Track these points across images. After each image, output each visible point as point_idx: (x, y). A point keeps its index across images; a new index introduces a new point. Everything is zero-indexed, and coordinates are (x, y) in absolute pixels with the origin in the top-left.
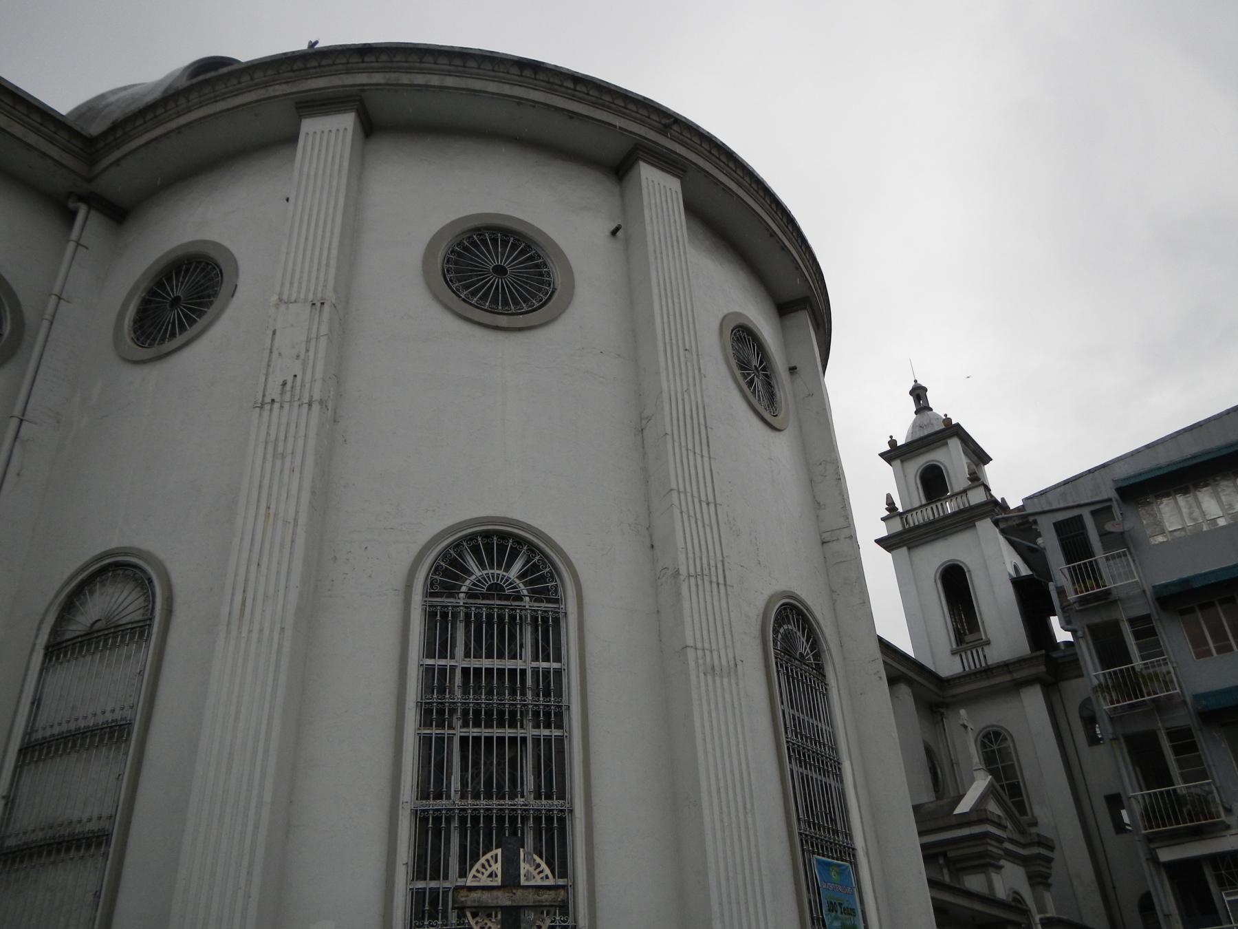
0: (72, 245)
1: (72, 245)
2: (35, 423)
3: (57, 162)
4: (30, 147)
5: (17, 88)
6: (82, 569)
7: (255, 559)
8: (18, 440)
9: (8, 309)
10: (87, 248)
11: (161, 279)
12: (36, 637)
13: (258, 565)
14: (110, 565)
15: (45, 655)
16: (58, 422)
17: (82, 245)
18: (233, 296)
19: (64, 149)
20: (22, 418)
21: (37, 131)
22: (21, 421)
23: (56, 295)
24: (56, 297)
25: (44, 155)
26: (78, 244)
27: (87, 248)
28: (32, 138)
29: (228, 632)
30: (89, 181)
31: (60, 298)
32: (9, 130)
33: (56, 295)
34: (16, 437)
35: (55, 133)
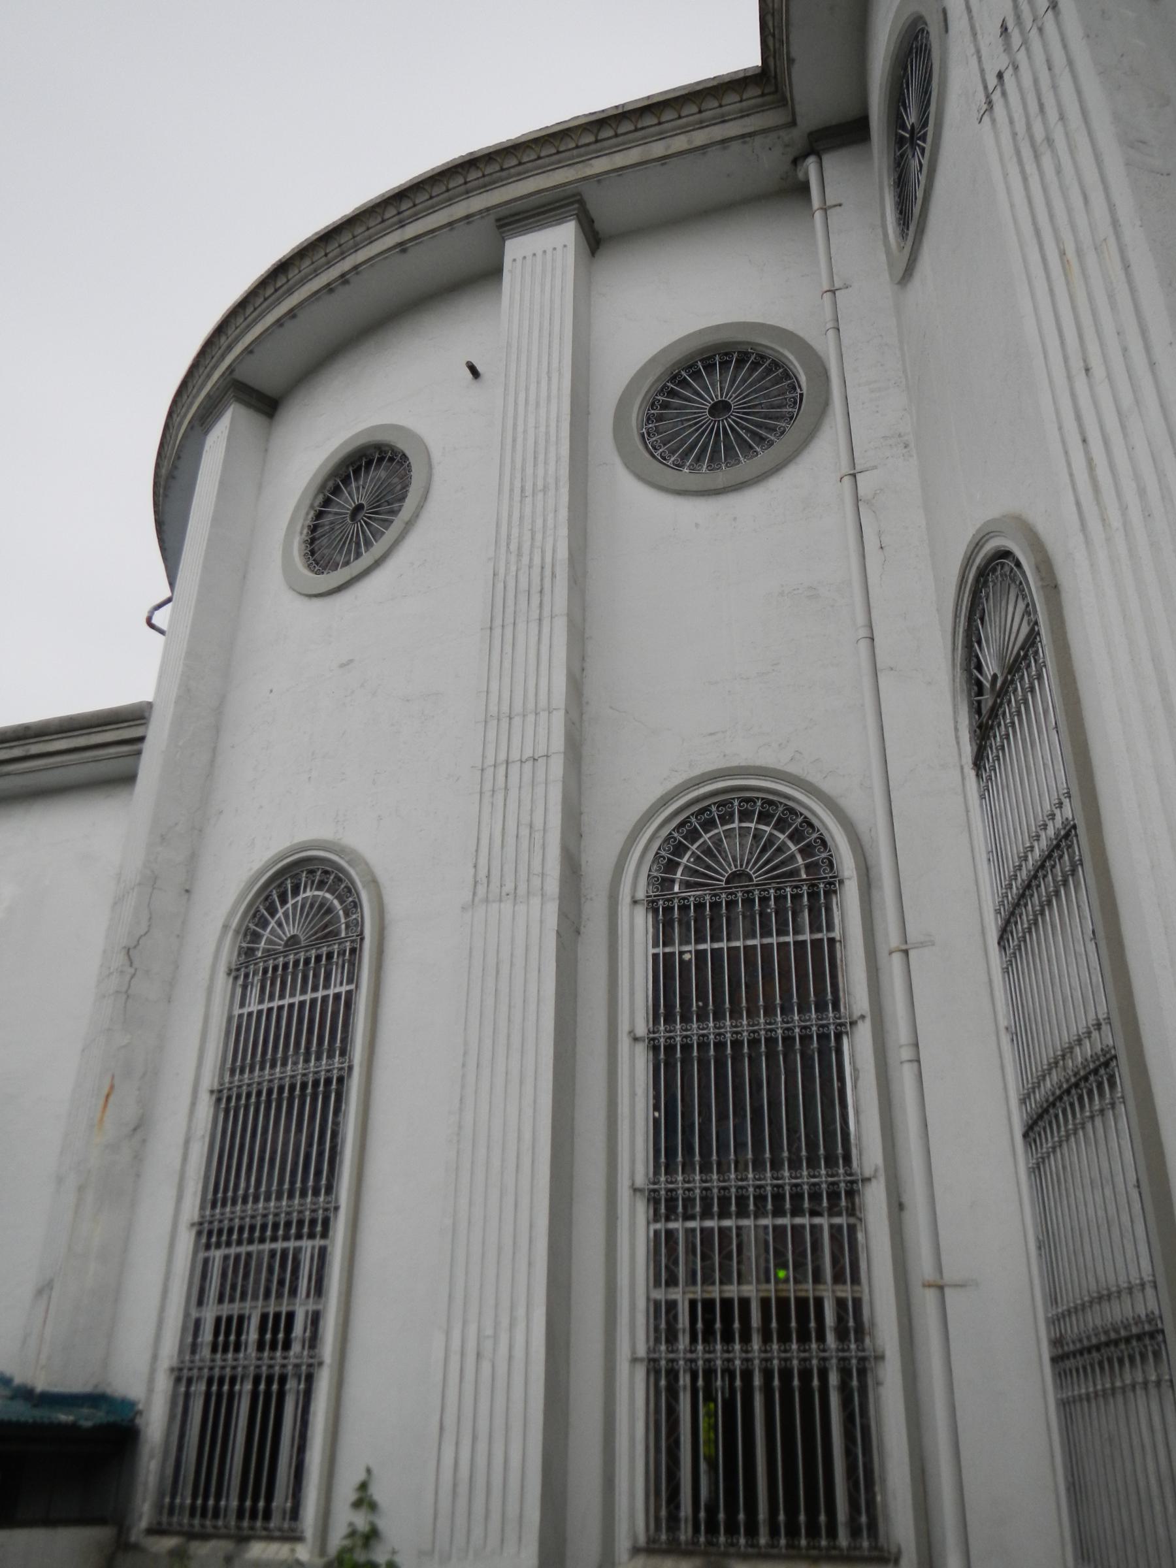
0: (818, 216)
1: (818, 216)
2: (875, 467)
3: (743, 136)
4: (703, 148)
5: (649, 97)
6: (956, 616)
7: (1077, 365)
8: (860, 503)
9: (791, 357)
10: (840, 205)
11: (896, 134)
12: (960, 755)
13: (1087, 370)
14: (977, 580)
15: (977, 775)
16: (906, 447)
17: (830, 207)
18: (947, 31)
19: (744, 114)
20: (852, 472)
21: (701, 125)
22: (854, 475)
23: (826, 292)
24: (828, 293)
25: (724, 142)
26: (825, 209)
27: (840, 205)
28: (700, 138)
29: (1088, 542)
30: (793, 123)
31: (833, 292)
32: (669, 152)
33: (826, 292)
34: (857, 500)
35: (721, 106)
